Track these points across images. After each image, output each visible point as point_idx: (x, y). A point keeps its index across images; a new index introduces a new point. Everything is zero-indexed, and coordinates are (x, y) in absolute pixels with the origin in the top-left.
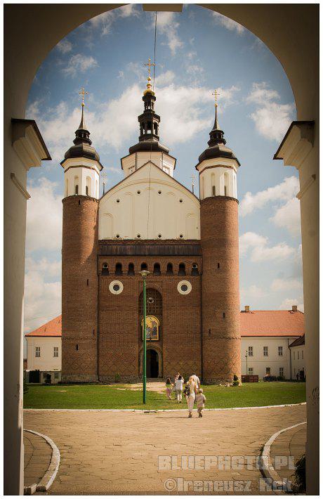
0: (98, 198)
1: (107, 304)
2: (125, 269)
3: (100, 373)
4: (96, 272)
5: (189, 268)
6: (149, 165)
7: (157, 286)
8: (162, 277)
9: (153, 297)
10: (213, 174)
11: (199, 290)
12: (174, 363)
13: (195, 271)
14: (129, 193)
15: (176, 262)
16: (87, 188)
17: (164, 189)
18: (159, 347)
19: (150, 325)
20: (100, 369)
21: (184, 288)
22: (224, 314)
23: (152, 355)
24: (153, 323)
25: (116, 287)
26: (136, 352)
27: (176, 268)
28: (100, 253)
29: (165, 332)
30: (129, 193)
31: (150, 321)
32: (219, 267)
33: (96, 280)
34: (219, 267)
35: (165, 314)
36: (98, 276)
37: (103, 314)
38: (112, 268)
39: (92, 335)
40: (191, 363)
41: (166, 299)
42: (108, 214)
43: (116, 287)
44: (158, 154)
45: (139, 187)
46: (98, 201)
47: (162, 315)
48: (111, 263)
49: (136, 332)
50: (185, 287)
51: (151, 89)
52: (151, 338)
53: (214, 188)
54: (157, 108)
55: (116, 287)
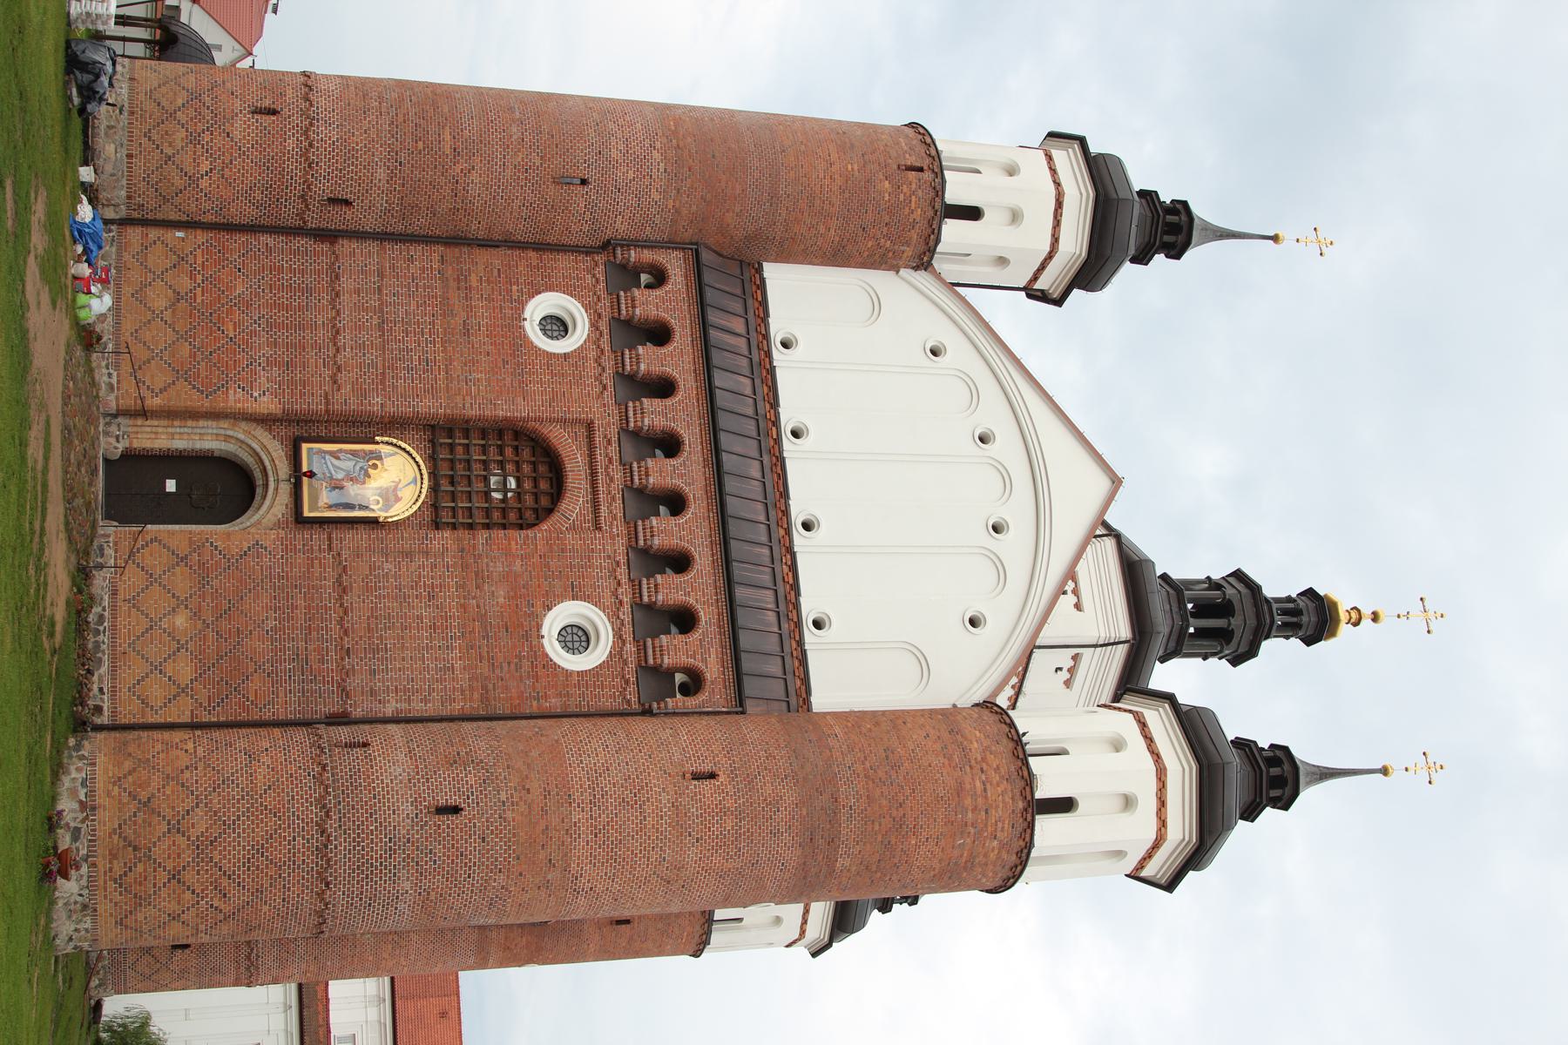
2: (649, 360)
3: (134, 234)
4: (621, 227)
5: (675, 650)
6: (1103, 484)
7: (575, 504)
8: (619, 528)
9: (519, 495)
10: (1118, 745)
11: (577, 706)
12: (182, 581)
14: (974, 393)
15: (695, 589)
17: (1015, 546)
18: (270, 519)
20: (154, 233)
21: (577, 638)
22: (456, 810)
23: (224, 488)
24: (390, 496)
26: (235, 399)
27: (670, 589)
28: (706, 256)
29: (350, 540)
30: (974, 393)
31: (393, 481)
32: (697, 777)
33: (579, 233)
34: (697, 777)
36: (607, 246)
37: (426, 258)
38: (647, 304)
39: (323, 189)
40: (184, 670)
41: (505, 552)
42: (877, 305)
43: (558, 318)
44: (1124, 631)
45: (1007, 446)
46: (924, 261)
47: (437, 525)
48: (666, 304)
49: (347, 400)
50: (579, 633)
51: (1344, 629)
52: (311, 474)
54: (1278, 650)
55: (557, 326)
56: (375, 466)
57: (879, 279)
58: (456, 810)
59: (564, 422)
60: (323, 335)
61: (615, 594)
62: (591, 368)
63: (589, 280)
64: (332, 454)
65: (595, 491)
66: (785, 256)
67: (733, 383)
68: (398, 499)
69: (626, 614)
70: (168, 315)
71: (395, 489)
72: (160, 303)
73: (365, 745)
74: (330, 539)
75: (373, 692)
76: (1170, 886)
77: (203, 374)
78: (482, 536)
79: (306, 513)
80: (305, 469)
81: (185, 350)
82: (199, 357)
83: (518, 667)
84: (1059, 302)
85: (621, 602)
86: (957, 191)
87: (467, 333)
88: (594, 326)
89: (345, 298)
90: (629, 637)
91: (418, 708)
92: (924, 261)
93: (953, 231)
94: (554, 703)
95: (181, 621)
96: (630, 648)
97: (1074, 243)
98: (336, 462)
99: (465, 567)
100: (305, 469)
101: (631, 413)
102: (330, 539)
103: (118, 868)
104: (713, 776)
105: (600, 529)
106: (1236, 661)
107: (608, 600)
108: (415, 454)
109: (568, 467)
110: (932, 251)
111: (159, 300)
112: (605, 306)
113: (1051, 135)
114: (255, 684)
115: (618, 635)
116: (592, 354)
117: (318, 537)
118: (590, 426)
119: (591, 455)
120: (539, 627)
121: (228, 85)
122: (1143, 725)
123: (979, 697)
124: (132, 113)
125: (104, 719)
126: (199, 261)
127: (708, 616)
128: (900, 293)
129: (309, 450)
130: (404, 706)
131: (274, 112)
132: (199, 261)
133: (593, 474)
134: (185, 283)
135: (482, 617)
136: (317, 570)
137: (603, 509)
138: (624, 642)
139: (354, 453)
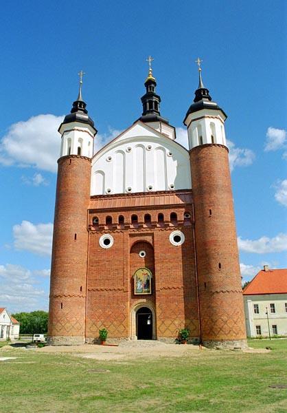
0: (90, 157)
7: (149, 239)
12: (168, 322)
14: (120, 151)
16: (79, 149)
17: (154, 145)
22: (220, 264)
25: (107, 242)
30: (120, 151)
35: (157, 267)
39: (78, 293)
44: (159, 122)
46: (90, 160)
47: (154, 269)
53: (201, 139)
55: (107, 242)
57: (93, 170)
58: (220, 264)
60: (110, 292)
66: (89, 191)
67: (118, 203)
73: (205, 284)
76: (226, 117)
78: (156, 258)
81: (115, 323)
84: (97, 131)
86: (75, 152)
88: (106, 233)
89: (102, 288)
92: (90, 160)
93: (83, 154)
95: (176, 322)
97: (87, 128)
103: (234, 334)
104: (210, 210)
106: (160, 101)
107: (169, 231)
110: (88, 158)
113: (59, 131)
123: (188, 154)
125: (198, 338)
127: (173, 211)
128: (97, 165)
134: (100, 323)
136: (164, 294)
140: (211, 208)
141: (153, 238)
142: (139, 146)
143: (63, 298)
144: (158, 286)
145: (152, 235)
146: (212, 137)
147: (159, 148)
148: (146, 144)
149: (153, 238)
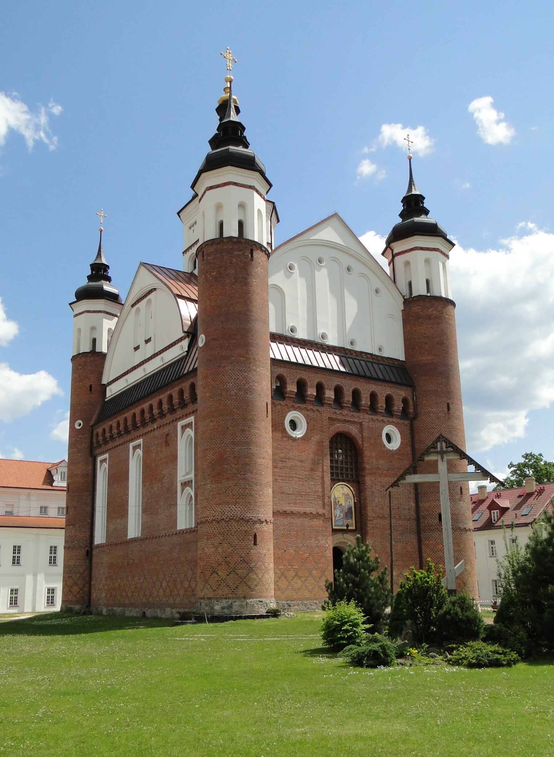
1: (282, 455)
7: (354, 430)
8: (361, 415)
10: (427, 261)
13: (405, 413)
19: (342, 502)
30: (306, 259)
35: (369, 480)
56: (338, 502)
59: (329, 428)
61: (379, 421)
62: (310, 413)
63: (279, 407)
64: (335, 517)
65: (350, 421)
68: (348, 494)
69: (386, 419)
70: (303, 579)
71: (345, 495)
72: (299, 581)
74: (370, 521)
75: (409, 510)
77: (321, 565)
79: (354, 528)
80: (345, 528)
81: (314, 572)
82: (317, 567)
83: (401, 459)
85: (382, 420)
87: (301, 461)
88: (295, 409)
90: (391, 420)
91: (412, 496)
94: (409, 449)
96: (394, 420)
98: (338, 516)
99: (375, 473)
100: (345, 528)
101: (329, 402)
102: (370, 521)
104: (448, 404)
105: (361, 422)
107: (381, 424)
108: (352, 489)
109: (341, 430)
111: (297, 583)
112: (290, 403)
114: (409, 549)
115: (390, 423)
116: (306, 413)
117: (370, 525)
118: (330, 419)
119: (339, 421)
120: (390, 450)
121: (243, 555)
122: (422, 249)
124: (261, 597)
126: (282, 567)
129: (335, 526)
130: (412, 500)
131: (255, 536)
132: (282, 567)
133: (345, 421)
134: (292, 573)
135: (388, 470)
137: (356, 420)
138: (393, 422)
139: (335, 509)
140: (449, 401)
141: (361, 431)
142: (334, 259)
143: (258, 526)
144: (370, 513)
145: (361, 424)
146: (428, 282)
147: (363, 275)
148: (347, 261)
149: (361, 431)
